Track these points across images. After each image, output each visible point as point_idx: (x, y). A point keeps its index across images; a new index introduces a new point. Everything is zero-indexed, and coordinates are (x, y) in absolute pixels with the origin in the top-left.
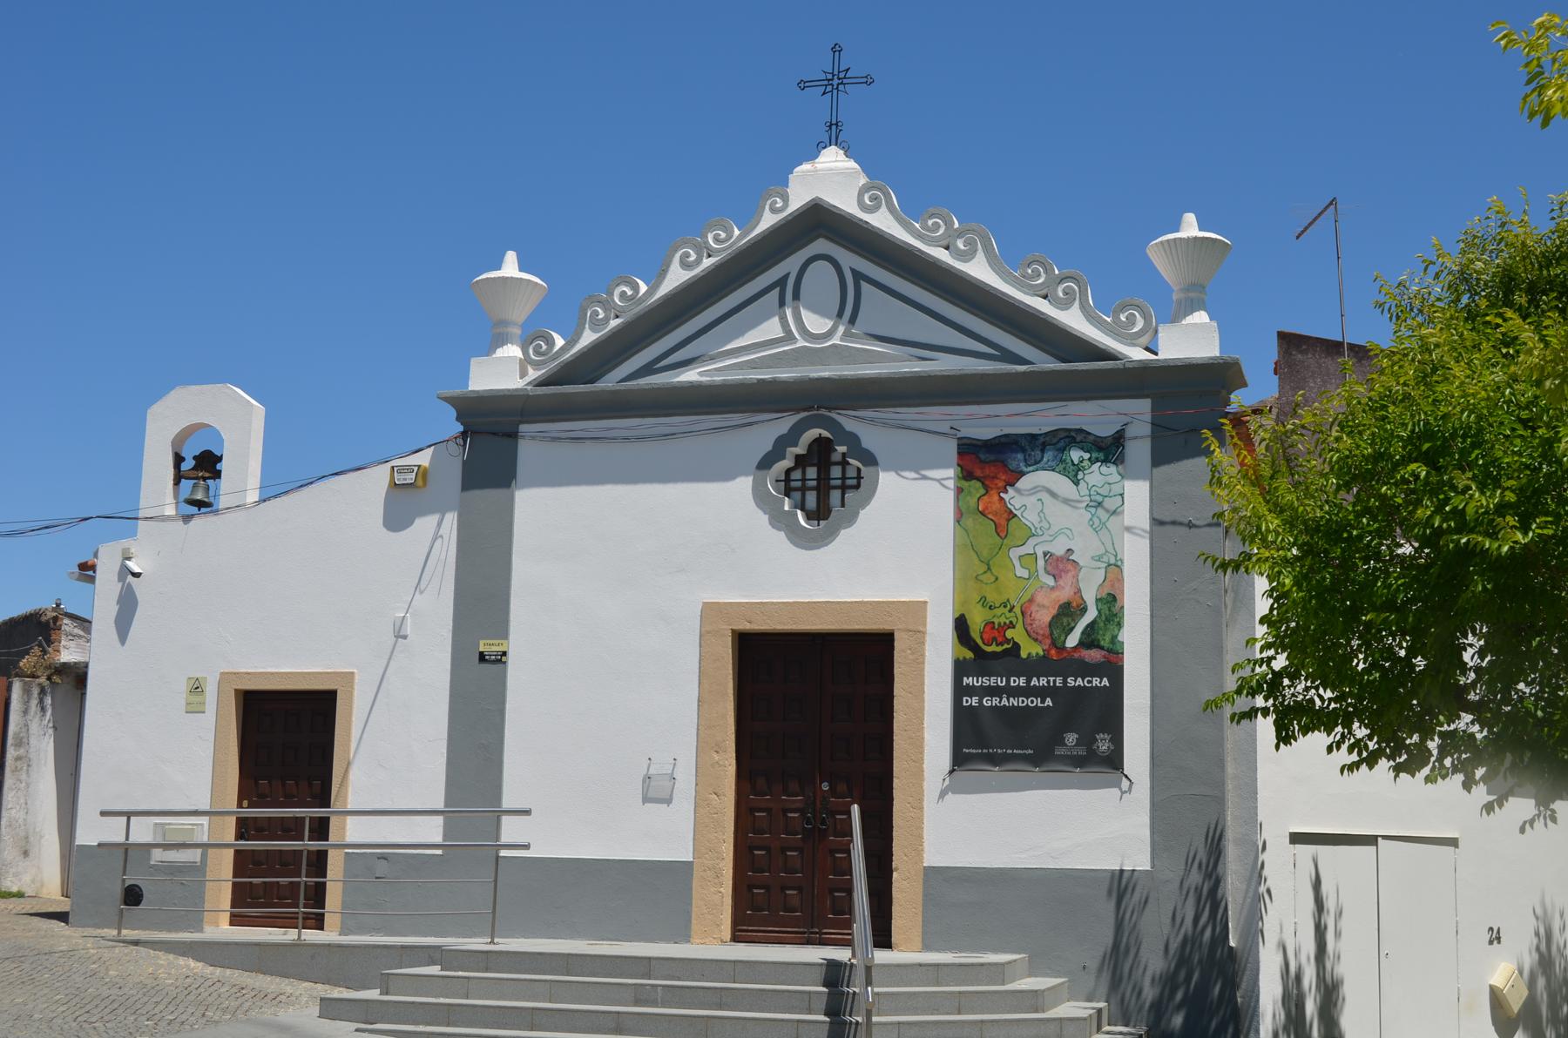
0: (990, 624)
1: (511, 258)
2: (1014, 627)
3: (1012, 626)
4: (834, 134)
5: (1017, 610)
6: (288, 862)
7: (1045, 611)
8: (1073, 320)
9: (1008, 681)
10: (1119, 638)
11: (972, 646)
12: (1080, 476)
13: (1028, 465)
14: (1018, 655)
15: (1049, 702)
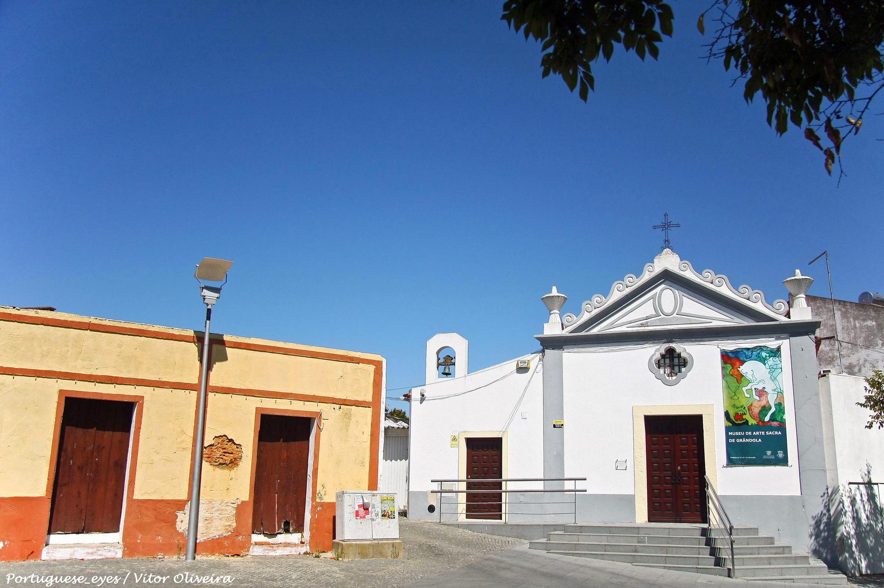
0: (737, 414)
1: (554, 289)
2: (746, 414)
3: (745, 414)
4: (667, 244)
5: (747, 408)
6: (486, 497)
7: (757, 409)
8: (760, 307)
9: (745, 433)
10: (784, 418)
11: (732, 422)
12: (766, 361)
13: (747, 359)
14: (748, 424)
15: (760, 440)
